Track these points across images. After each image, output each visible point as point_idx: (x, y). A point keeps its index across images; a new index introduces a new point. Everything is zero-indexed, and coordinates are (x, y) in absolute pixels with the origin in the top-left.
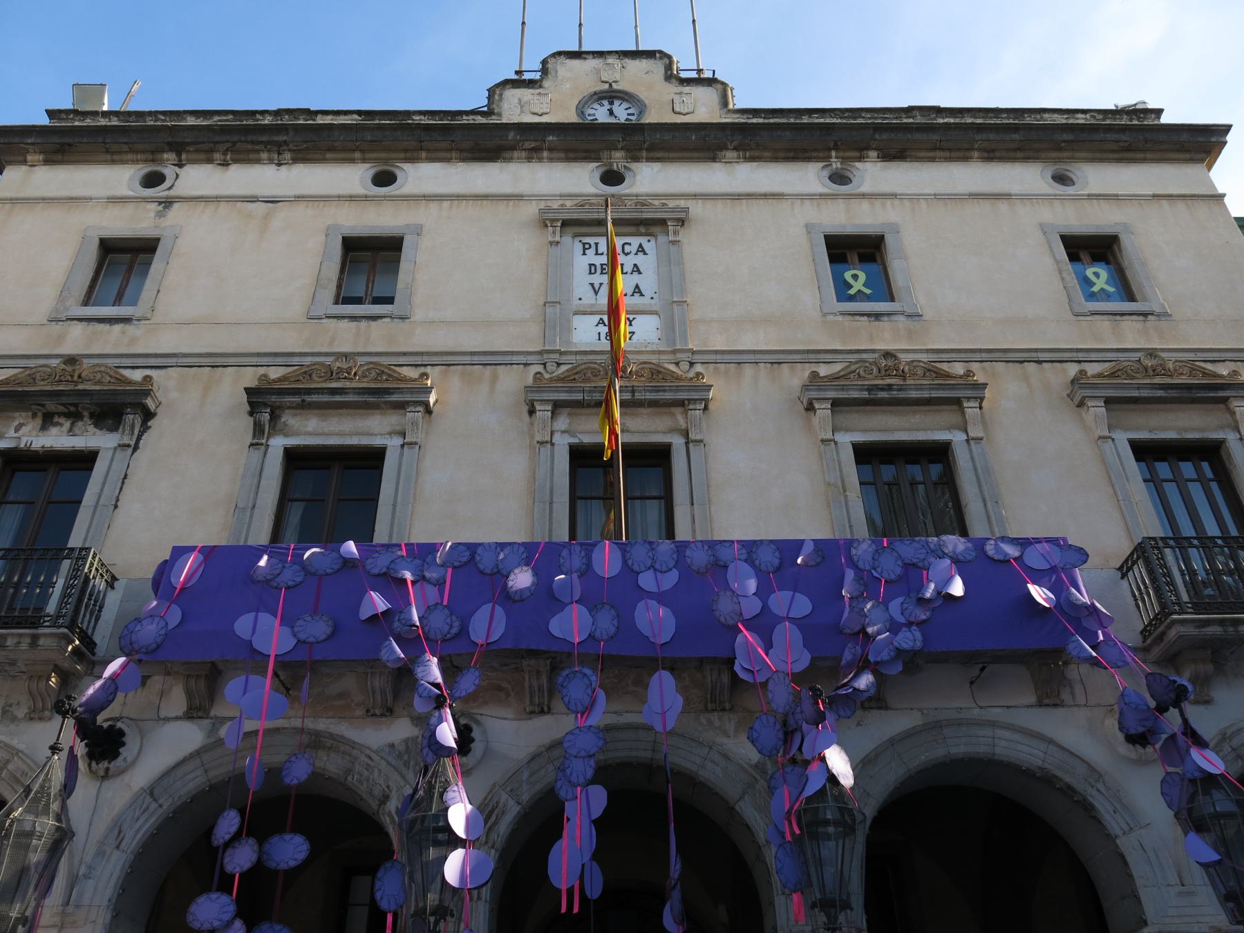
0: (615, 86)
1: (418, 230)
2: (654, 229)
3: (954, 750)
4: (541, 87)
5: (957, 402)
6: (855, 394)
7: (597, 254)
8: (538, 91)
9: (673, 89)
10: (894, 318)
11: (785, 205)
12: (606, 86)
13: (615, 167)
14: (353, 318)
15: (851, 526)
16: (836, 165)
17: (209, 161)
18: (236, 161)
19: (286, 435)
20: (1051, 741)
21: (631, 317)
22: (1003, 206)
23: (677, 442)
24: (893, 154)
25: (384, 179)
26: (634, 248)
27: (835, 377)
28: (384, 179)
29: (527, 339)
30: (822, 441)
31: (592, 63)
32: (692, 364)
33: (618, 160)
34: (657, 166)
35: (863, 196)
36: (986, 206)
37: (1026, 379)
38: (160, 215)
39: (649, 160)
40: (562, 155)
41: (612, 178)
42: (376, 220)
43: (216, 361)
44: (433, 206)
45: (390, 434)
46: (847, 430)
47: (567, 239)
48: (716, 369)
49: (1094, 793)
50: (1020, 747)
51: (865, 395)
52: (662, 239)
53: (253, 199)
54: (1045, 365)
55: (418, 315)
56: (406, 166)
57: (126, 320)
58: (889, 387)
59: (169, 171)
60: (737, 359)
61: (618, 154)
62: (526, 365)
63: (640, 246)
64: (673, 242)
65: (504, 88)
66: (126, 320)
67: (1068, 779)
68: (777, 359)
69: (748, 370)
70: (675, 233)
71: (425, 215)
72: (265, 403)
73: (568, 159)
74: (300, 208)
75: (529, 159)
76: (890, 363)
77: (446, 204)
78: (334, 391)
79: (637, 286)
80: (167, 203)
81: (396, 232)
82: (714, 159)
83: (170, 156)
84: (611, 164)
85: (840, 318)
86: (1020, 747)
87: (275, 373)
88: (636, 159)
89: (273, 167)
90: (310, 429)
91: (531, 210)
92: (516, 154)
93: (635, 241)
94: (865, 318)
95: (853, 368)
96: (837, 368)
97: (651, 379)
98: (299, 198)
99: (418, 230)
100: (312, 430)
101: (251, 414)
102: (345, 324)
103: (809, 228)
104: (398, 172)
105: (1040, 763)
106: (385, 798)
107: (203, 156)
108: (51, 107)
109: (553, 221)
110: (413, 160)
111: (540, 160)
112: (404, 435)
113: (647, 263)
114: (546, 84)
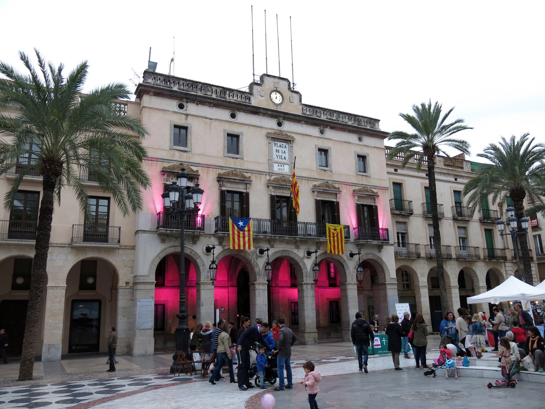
5: (336, 194)
9: (290, 93)
11: (312, 138)
14: (233, 158)
16: (322, 128)
22: (349, 145)
24: (332, 128)
26: (284, 146)
28: (233, 116)
33: (281, 120)
36: (346, 144)
37: (347, 189)
38: (186, 119)
41: (280, 124)
44: (245, 126)
53: (206, 118)
56: (237, 112)
57: (186, 152)
59: (185, 104)
61: (281, 118)
66: (186, 152)
68: (309, 179)
72: (220, 179)
74: (217, 122)
78: (234, 179)
81: (238, 134)
83: (185, 100)
87: (222, 172)
91: (264, 132)
93: (285, 144)
98: (216, 119)
102: (231, 159)
113: (286, 150)
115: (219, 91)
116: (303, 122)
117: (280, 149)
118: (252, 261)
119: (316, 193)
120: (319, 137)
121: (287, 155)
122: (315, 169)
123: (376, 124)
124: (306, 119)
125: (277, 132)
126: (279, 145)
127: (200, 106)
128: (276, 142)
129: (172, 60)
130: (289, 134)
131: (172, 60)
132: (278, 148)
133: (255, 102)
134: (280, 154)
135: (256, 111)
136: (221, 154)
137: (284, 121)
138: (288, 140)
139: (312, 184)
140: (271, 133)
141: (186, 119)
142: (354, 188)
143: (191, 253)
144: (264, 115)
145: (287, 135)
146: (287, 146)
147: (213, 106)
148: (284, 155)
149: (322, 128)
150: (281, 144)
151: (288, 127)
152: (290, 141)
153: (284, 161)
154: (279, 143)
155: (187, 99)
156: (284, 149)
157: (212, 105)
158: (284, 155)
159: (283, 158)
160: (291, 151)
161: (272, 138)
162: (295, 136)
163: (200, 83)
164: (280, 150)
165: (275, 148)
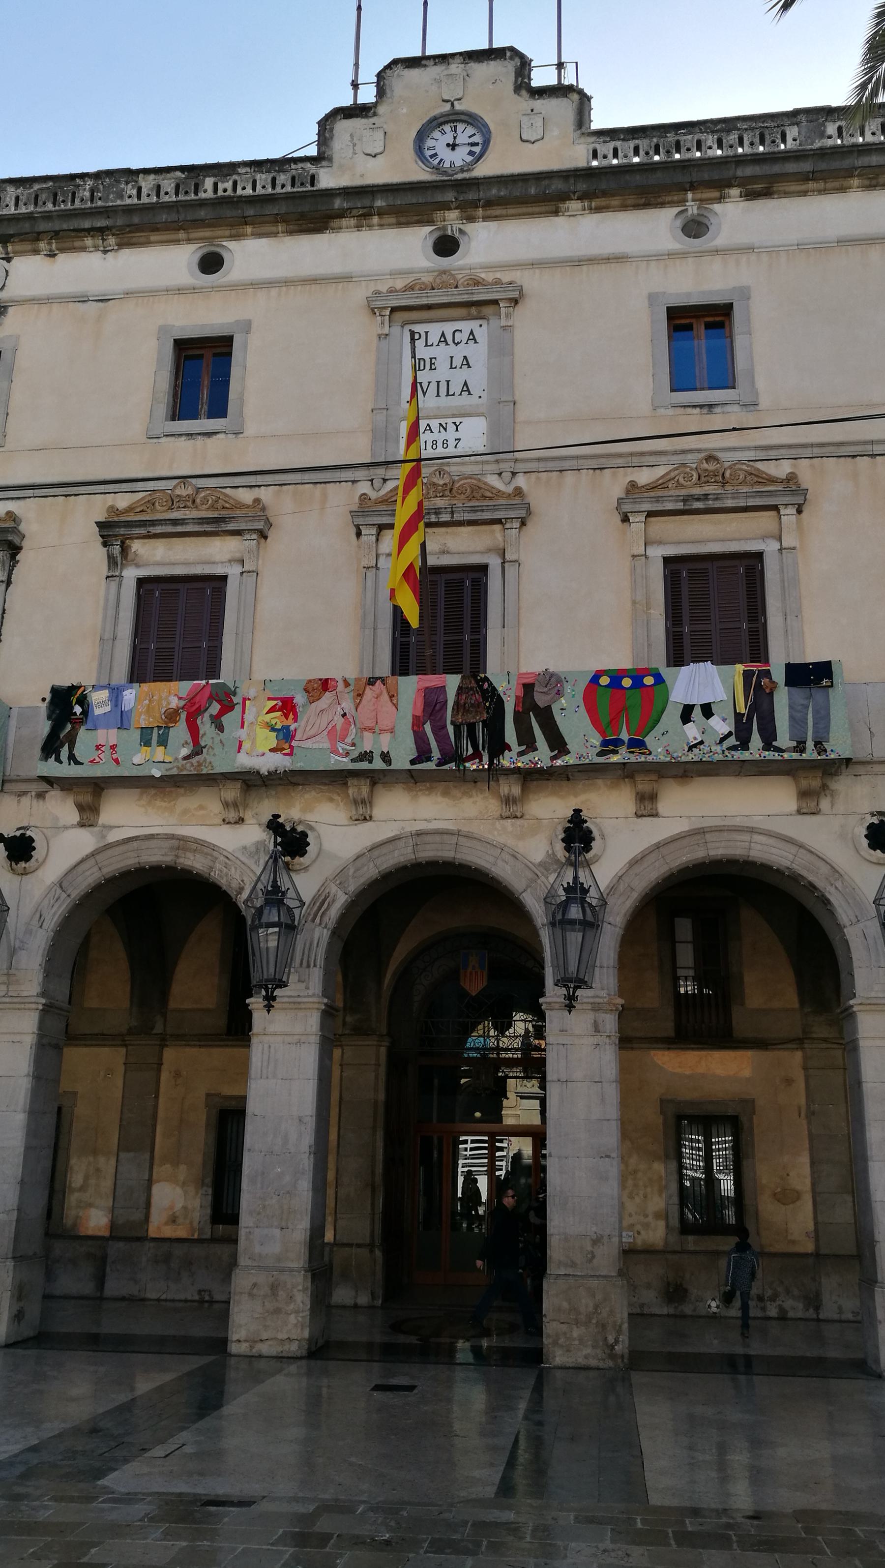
0: (458, 107)
1: (247, 327)
2: (488, 310)
3: (712, 853)
4: (375, 114)
6: (670, 506)
7: (426, 345)
8: (372, 120)
9: (525, 103)
10: (728, 408)
12: (447, 107)
13: (449, 233)
14: (190, 435)
15: (649, 645)
16: (692, 208)
17: (36, 252)
18: (62, 250)
19: (137, 566)
20: (801, 846)
21: (458, 421)
23: (494, 562)
24: (760, 189)
26: (462, 337)
27: (653, 487)
28: (211, 263)
30: (634, 556)
31: (434, 71)
32: (514, 474)
34: (493, 225)
35: (716, 251)
39: (485, 218)
40: (393, 220)
41: (446, 246)
42: (203, 318)
43: (68, 488)
44: (261, 295)
45: (230, 561)
46: (660, 543)
48: (538, 478)
49: (833, 890)
50: (774, 851)
51: (680, 506)
52: (494, 322)
53: (83, 299)
54: (878, 457)
55: (251, 429)
56: (231, 245)
58: (706, 497)
61: (453, 215)
62: (354, 482)
63: (472, 333)
64: (504, 328)
65: (334, 123)
67: (811, 878)
69: (569, 477)
70: (508, 316)
71: (250, 308)
72: (114, 533)
73: (399, 224)
75: (359, 227)
76: (711, 467)
77: (274, 292)
78: (175, 522)
79: (466, 384)
82: (556, 213)
84: (444, 228)
85: (671, 412)
86: (774, 851)
87: (123, 501)
88: (471, 219)
89: (99, 254)
90: (158, 558)
91: (360, 294)
92: (344, 222)
93: (466, 326)
94: (698, 410)
95: (673, 474)
96: (660, 471)
97: (472, 498)
99: (247, 327)
100: (160, 557)
101: (105, 544)
102: (182, 442)
103: (652, 298)
105: (788, 864)
106: (241, 890)
107: (28, 246)
110: (237, 237)
111: (370, 227)
112: (242, 562)
113: (478, 353)
114: (381, 109)
115: (168, 185)
117: (442, 353)
119: (637, 520)
120: (672, 255)
121: (478, 377)
124: (582, 186)
125: (427, 279)
126: (434, 338)
127: (61, 257)
130: (489, 277)
137: (469, 228)
139: (614, 486)
140: (392, 291)
145: (477, 283)
148: (457, 378)
149: (692, 208)
150: (448, 328)
151: (491, 244)
152: (495, 302)
154: (435, 330)
156: (459, 353)
159: (456, 388)
160: (502, 350)
161: (394, 310)
162: (528, 280)
163: (83, 176)
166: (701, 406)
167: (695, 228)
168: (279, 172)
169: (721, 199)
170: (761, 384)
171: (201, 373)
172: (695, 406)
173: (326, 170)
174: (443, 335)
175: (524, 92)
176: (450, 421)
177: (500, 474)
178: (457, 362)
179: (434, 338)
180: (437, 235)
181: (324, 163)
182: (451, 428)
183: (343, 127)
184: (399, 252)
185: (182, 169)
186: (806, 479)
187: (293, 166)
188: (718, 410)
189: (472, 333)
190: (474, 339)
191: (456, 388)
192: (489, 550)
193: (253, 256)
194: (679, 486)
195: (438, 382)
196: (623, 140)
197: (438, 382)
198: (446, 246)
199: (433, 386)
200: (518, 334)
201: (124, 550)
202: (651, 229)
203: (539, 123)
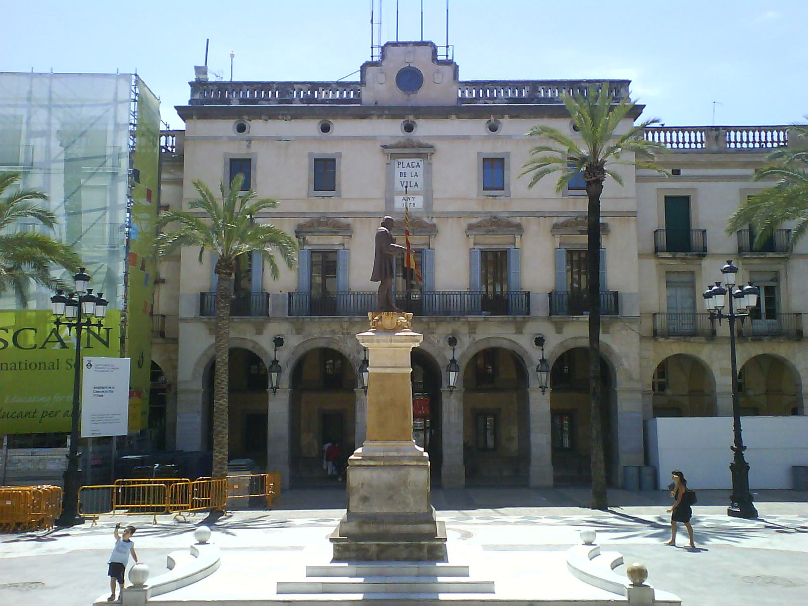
0: (411, 65)
1: (340, 155)
4: (381, 65)
8: (380, 68)
10: (501, 198)
17: (261, 119)
21: (413, 196)
25: (326, 128)
28: (326, 128)
29: (377, 206)
31: (401, 49)
32: (432, 217)
38: (248, 147)
41: (409, 128)
42: (326, 150)
47: (393, 161)
52: (426, 161)
55: (345, 195)
59: (248, 123)
60: (448, 215)
68: (459, 215)
70: (431, 159)
75: (378, 118)
79: (416, 183)
80: (249, 141)
87: (302, 221)
89: (284, 121)
93: (416, 160)
94: (491, 197)
96: (479, 219)
100: (316, 241)
104: (330, 124)
106: (350, 355)
108: (190, 81)
109: (387, 153)
113: (420, 171)
114: (383, 64)
116: (454, 117)
117: (408, 170)
118: (351, 357)
121: (420, 180)
122: (474, 195)
123: (622, 90)
126: (405, 164)
127: (270, 121)
128: (400, 160)
129: (232, 56)
131: (232, 56)
132: (403, 170)
133: (367, 96)
134: (408, 178)
135: (364, 113)
136: (304, 193)
137: (417, 121)
138: (423, 152)
139: (464, 223)
141: (248, 147)
142: (555, 220)
143: (253, 347)
144: (380, 116)
146: (421, 164)
147: (292, 119)
150: (410, 161)
151: (425, 129)
153: (416, 189)
154: (406, 161)
155: (248, 114)
157: (289, 117)
158: (414, 180)
159: (413, 184)
160: (428, 171)
164: (410, 171)
165: (397, 171)
166: (492, 196)
167: (493, 128)
168: (347, 87)
169: (503, 118)
170: (512, 189)
171: (324, 174)
172: (491, 196)
173: (364, 88)
174: (408, 164)
175: (435, 62)
176: (411, 196)
177: (428, 217)
178: (414, 175)
179: (405, 164)
180: (406, 123)
181: (363, 85)
182: (411, 199)
183: (370, 69)
184: (392, 129)
185: (310, 83)
186: (524, 224)
187: (352, 85)
188: (497, 198)
189: (418, 164)
190: (419, 166)
191: (413, 184)
192: (424, 244)
193: (341, 127)
194: (485, 226)
195: (407, 182)
196: (470, 86)
197: (407, 182)
198: (409, 128)
199: (406, 183)
200: (434, 165)
201: (304, 239)
202: (477, 127)
203: (440, 76)
